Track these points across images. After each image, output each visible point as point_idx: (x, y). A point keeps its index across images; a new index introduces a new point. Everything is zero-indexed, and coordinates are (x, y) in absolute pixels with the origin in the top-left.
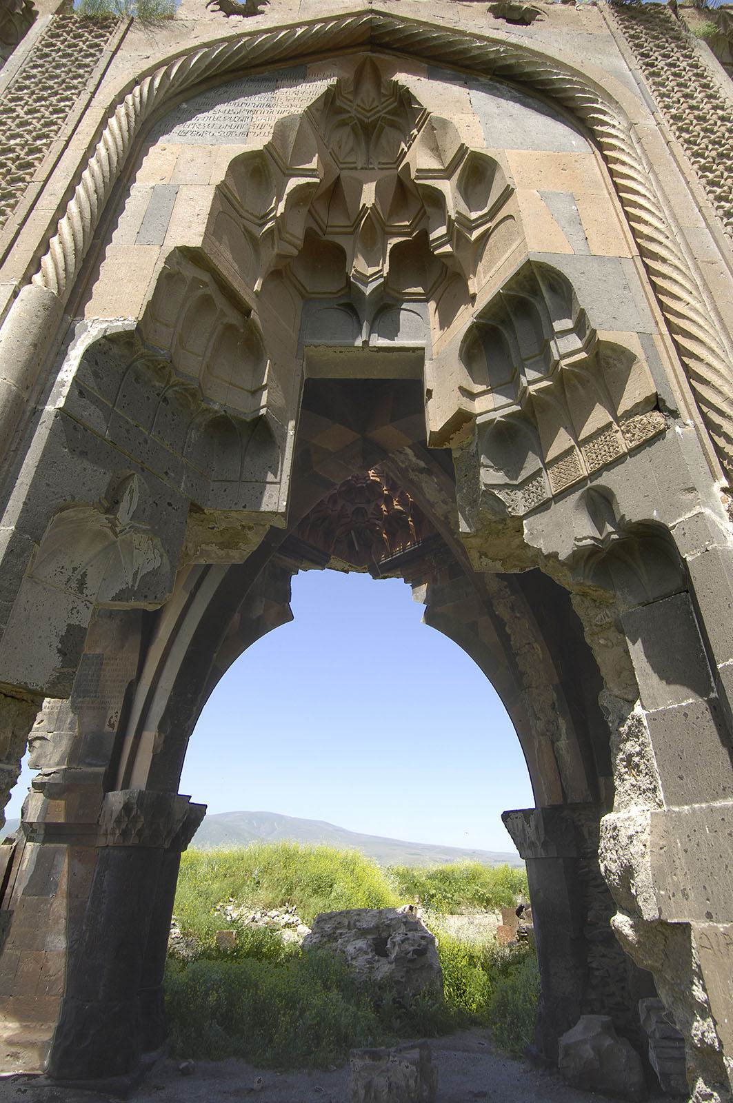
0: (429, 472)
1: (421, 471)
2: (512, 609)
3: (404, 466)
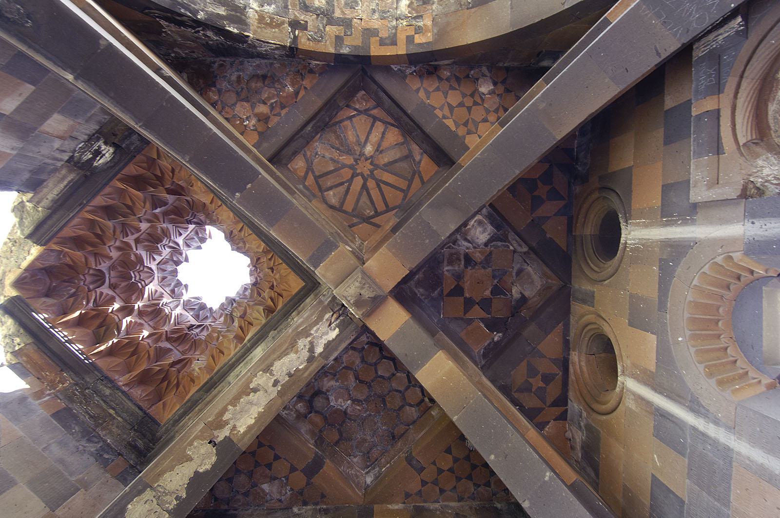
0: (311, 359)
1: (311, 350)
3: (312, 332)
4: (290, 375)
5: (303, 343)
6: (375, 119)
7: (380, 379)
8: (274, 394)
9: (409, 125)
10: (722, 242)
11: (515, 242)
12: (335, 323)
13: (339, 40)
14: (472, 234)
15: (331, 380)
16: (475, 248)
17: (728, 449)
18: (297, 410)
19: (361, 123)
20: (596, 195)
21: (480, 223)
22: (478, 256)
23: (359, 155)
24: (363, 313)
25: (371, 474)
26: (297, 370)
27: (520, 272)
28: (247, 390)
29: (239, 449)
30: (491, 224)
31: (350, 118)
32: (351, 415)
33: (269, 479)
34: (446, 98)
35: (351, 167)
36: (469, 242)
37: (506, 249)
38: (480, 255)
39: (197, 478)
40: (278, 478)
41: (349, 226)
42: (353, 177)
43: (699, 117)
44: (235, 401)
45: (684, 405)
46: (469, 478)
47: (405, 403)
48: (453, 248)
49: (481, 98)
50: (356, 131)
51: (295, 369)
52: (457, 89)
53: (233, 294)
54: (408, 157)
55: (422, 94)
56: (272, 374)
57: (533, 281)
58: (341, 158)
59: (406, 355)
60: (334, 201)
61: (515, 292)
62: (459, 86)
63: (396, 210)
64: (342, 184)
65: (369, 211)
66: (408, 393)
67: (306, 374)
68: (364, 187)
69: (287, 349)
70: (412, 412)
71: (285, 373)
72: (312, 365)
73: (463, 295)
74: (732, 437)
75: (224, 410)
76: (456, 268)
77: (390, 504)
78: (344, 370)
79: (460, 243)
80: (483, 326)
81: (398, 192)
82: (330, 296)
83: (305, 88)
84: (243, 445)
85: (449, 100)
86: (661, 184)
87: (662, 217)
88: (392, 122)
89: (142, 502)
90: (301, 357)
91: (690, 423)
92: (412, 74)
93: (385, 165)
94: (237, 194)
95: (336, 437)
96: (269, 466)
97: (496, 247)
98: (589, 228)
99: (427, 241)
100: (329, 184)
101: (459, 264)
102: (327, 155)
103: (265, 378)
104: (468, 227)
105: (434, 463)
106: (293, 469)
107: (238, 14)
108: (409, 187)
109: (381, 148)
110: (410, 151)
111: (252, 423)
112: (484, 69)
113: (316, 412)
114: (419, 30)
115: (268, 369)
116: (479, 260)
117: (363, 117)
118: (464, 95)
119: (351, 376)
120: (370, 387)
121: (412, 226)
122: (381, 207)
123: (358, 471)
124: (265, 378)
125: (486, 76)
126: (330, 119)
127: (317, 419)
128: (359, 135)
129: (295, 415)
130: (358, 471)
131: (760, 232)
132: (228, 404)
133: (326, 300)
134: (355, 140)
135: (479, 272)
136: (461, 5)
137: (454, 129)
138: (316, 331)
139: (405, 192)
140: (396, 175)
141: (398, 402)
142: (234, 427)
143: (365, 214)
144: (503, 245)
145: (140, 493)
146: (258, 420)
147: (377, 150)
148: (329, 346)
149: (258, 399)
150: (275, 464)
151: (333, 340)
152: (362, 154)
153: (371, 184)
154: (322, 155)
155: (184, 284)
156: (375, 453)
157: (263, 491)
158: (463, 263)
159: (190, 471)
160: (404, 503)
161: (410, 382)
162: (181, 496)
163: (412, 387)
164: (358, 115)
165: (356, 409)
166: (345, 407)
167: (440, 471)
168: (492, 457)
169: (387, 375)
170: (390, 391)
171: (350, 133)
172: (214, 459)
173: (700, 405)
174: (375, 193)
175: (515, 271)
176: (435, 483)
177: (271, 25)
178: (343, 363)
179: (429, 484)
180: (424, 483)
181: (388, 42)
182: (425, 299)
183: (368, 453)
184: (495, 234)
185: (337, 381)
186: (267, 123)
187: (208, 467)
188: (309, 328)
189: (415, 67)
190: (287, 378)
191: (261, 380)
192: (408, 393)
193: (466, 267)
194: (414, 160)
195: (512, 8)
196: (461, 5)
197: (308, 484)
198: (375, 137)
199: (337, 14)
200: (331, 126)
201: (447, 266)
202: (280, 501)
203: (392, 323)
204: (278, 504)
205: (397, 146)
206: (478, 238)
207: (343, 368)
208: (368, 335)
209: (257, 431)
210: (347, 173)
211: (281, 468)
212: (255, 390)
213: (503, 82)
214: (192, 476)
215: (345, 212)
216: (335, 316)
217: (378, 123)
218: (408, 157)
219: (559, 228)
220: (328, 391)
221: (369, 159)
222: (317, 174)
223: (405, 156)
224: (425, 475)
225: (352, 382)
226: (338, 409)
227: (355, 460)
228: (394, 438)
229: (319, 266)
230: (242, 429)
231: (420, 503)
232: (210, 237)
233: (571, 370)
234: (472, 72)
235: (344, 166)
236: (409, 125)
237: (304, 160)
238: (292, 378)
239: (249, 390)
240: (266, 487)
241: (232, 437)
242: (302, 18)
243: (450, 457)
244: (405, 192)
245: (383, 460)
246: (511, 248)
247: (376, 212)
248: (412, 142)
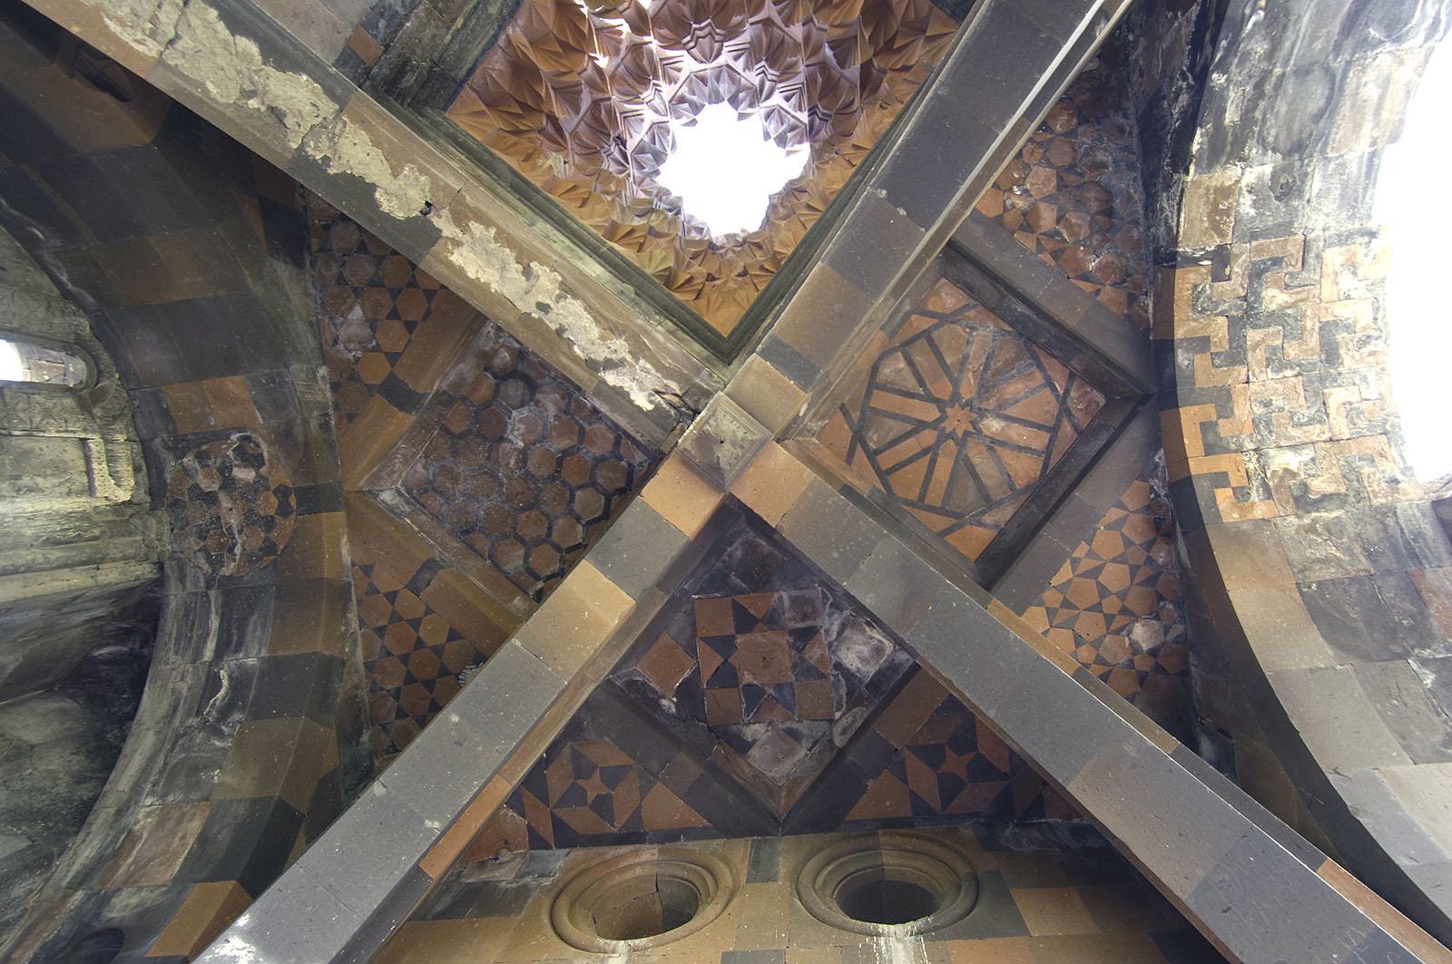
0: (592, 365)
1: (609, 364)
2: (277, 114)
3: (642, 362)
4: (560, 331)
5: (620, 347)
6: (1054, 430)
8: (523, 307)
9: (1051, 495)
12: (662, 402)
13: (1202, 344)
14: (855, 638)
15: (556, 405)
16: (830, 645)
18: (496, 351)
19: (1044, 405)
20: (962, 869)
21: (878, 650)
22: (814, 653)
23: (979, 409)
24: (689, 452)
25: (397, 500)
26: (570, 343)
27: (793, 734)
28: (525, 258)
29: (421, 256)
30: (878, 673)
31: (1050, 384)
32: (497, 450)
33: (370, 316)
34: (1114, 561)
35: (955, 397)
36: (840, 633)
37: (835, 704)
38: (818, 656)
39: (362, 189)
40: (374, 332)
41: (843, 405)
42: (937, 401)
44: (504, 238)
46: (410, 679)
47: (530, 546)
48: (825, 604)
49: (1122, 629)
50: (1027, 397)
51: (572, 338)
52: (1132, 581)
53: (687, 209)
54: (989, 503)
55: (1114, 514)
56: (559, 298)
57: (779, 761)
58: (970, 375)
59: (620, 539)
60: (887, 371)
61: (755, 731)
62: (1140, 584)
63: (883, 490)
64: (921, 382)
65: (874, 438)
66: (546, 549)
67: (564, 360)
68: (921, 425)
69: (606, 319)
70: (514, 560)
71: (565, 322)
72: (582, 368)
73: (738, 632)
75: (487, 222)
76: (787, 615)
77: (350, 541)
78: (577, 427)
79: (836, 616)
80: (686, 675)
81: (918, 490)
82: (707, 384)
83: (1098, 292)
84: (429, 264)
85: (1110, 567)
88: (1053, 463)
89: (314, 100)
90: (593, 348)
92: (1152, 490)
93: (967, 460)
94: (884, 192)
95: (457, 429)
96: (394, 315)
97: (836, 686)
98: (894, 860)
99: (836, 555)
100: (918, 359)
101: (794, 619)
102: (973, 349)
103: (550, 287)
104: (867, 629)
105: (429, 611)
106: (393, 358)
107: (1228, 149)
108: (931, 509)
109: (998, 448)
110: (1000, 503)
111: (469, 274)
112: (1178, 629)
113: (497, 387)
114: (1241, 494)
115: (566, 290)
116: (807, 656)
117: (1053, 407)
118: (1122, 595)
119: (567, 441)
120: (552, 478)
121: (861, 522)
122: (886, 460)
123: (400, 475)
124: (550, 287)
125: (1165, 635)
126: (1041, 346)
127: (484, 391)
128: (1019, 404)
129: (487, 349)
130: (400, 475)
132: (497, 226)
133: (702, 380)
134: (1008, 396)
135: (785, 659)
137: (1055, 581)
138: (644, 370)
139: (920, 503)
140: (949, 483)
141: (530, 533)
142: (458, 244)
143: (868, 432)
144: (841, 699)
145: (329, 92)
146: (476, 284)
147: (994, 441)
148: (621, 394)
149: (512, 279)
150: (397, 325)
151: (631, 402)
152: (982, 413)
153: (928, 437)
154: (971, 339)
155: (697, 117)
156: (435, 502)
157: (350, 309)
158: (799, 625)
159: (374, 175)
160: (353, 565)
161: (569, 550)
162: (329, 166)
163: (559, 555)
164: (1057, 396)
165: (510, 458)
166: (511, 437)
167: (416, 624)
168: (455, 719)
169: (577, 507)
170: (548, 516)
171: (1020, 386)
172: (400, 215)
174: (910, 446)
175: (795, 726)
176: (395, 618)
177: (1214, 211)
178: (590, 424)
179: (390, 607)
180: (392, 597)
181: (1211, 438)
182: (724, 562)
183: (434, 489)
184: (861, 682)
185: (556, 417)
186: (1022, 228)
187: (385, 207)
188: (648, 354)
189: (1166, 495)
190: (554, 327)
191: (547, 281)
192: (546, 549)
193: (791, 632)
194: (983, 513)
195: (1311, 670)
196: (1302, 571)
197: (370, 388)
198: (1019, 434)
199: (1253, 335)
200: (1028, 350)
201: (790, 597)
202: (336, 342)
203: (675, 506)
204: (328, 337)
205: (1005, 476)
206: (848, 649)
207: (581, 427)
208: (646, 465)
209: (454, 284)
210: (943, 389)
211: (394, 336)
212: (527, 272)
213: (1158, 668)
214: (367, 181)
215: (869, 394)
216: (675, 400)
217: (1046, 437)
218: (989, 503)
219: (888, 803)
220: (537, 403)
221: (975, 428)
222: (935, 335)
223: (989, 496)
224: (406, 598)
225: (558, 444)
226: (506, 425)
227: (419, 468)
228: (466, 532)
229: (766, 358)
230: (456, 258)
231: (356, 594)
232: (789, 153)
233: (623, 850)
234: (1170, 606)
235: (955, 383)
236: (1051, 495)
237: (957, 307)
238: (556, 336)
239: (526, 261)
240: (357, 313)
241: (441, 242)
242: (1236, 269)
243: (441, 639)
244: (920, 503)
245: (424, 518)
246: (838, 715)
247: (877, 452)
248: (1017, 505)
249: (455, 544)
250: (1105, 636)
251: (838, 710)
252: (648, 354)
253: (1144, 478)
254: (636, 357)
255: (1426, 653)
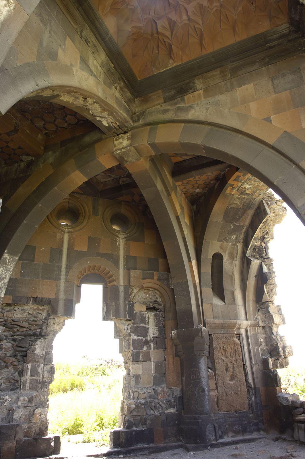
7: (64, 115)
10: (118, 278)
11: (126, 180)
12: (111, 124)
17: (60, 279)
43: (153, 274)
45: (67, 263)
62: (204, 185)
67: (85, 114)
74: (64, 281)
86: (137, 256)
87: (127, 256)
91: (62, 265)
98: (123, 211)
99: (142, 184)
105: (12, 141)
112: (205, 192)
114: (233, 189)
118: (199, 185)
131: (121, 290)
136: (230, 204)
137: (187, 180)
148: (100, 122)
151: (102, 124)
163: (56, 127)
167: (7, 142)
168: (40, 205)
169: (67, 119)
173: (70, 269)
194: (183, 156)
195: (216, 222)
196: (230, 204)
213: (197, 195)
216: (116, 126)
246: (123, 176)
249: (19, 116)
250: (190, 189)
251: (123, 175)
252: (113, 116)
253: (221, 171)
254: (109, 115)
255: (235, 223)
